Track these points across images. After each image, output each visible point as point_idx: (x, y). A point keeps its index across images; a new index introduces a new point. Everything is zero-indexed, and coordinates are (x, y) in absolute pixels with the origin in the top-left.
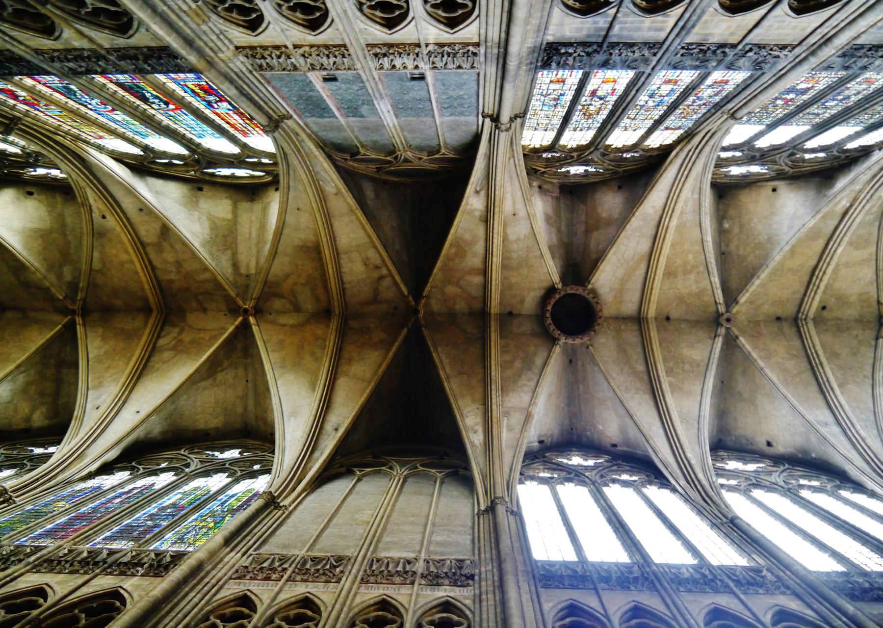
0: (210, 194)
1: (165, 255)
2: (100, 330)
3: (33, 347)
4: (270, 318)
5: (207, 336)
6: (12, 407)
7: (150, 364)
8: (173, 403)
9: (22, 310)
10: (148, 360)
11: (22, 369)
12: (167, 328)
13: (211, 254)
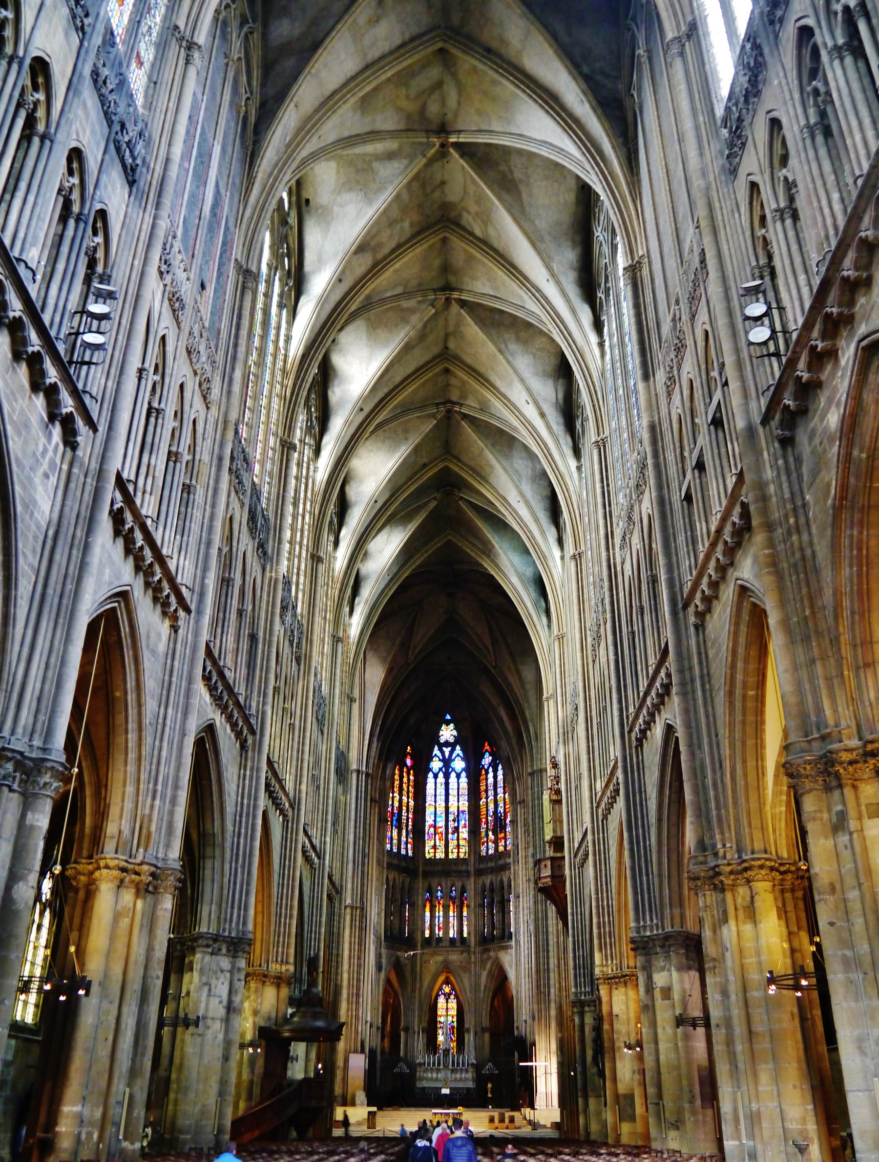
0: (311, 190)
1: (384, 240)
2: (466, 279)
3: (481, 334)
4: (450, 116)
5: (471, 189)
6: (539, 353)
7: (501, 250)
8: (542, 240)
9: (447, 336)
10: (496, 251)
11: (503, 346)
12: (463, 222)
13: (379, 190)
